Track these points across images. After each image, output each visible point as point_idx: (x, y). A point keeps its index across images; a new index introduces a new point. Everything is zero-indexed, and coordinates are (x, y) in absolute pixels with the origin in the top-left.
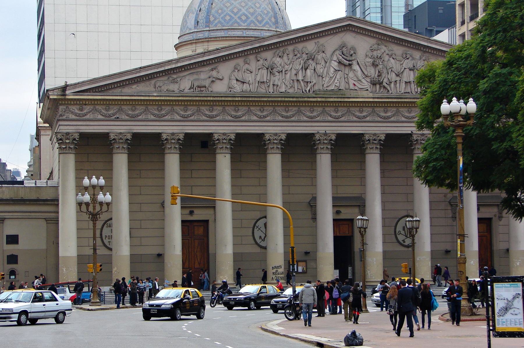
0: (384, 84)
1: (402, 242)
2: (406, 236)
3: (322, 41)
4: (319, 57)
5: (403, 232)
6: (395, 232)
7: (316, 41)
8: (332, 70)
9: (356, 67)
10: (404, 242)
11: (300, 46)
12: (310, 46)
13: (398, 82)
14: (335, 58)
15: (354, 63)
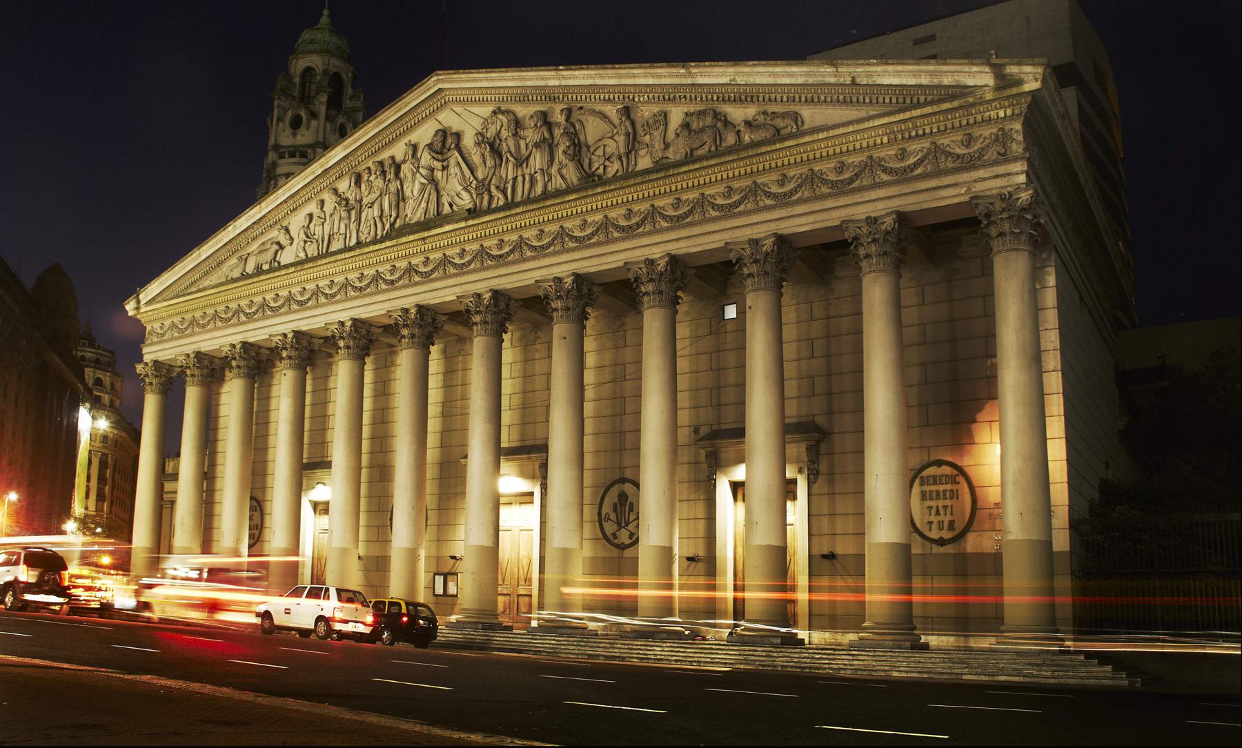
0: (493, 189)
1: (611, 538)
2: (619, 525)
3: (413, 137)
4: (406, 169)
5: (613, 516)
6: (599, 514)
7: (406, 140)
8: (417, 186)
9: (453, 170)
10: (615, 538)
11: (385, 155)
12: (399, 150)
13: (520, 179)
14: (423, 162)
15: (452, 161)
